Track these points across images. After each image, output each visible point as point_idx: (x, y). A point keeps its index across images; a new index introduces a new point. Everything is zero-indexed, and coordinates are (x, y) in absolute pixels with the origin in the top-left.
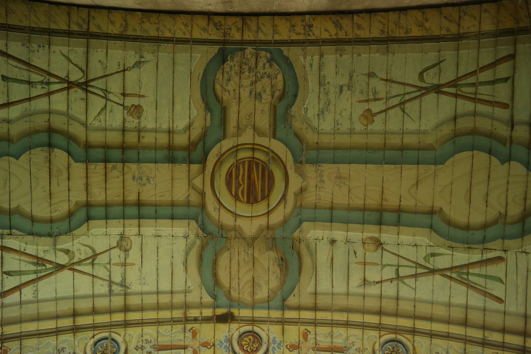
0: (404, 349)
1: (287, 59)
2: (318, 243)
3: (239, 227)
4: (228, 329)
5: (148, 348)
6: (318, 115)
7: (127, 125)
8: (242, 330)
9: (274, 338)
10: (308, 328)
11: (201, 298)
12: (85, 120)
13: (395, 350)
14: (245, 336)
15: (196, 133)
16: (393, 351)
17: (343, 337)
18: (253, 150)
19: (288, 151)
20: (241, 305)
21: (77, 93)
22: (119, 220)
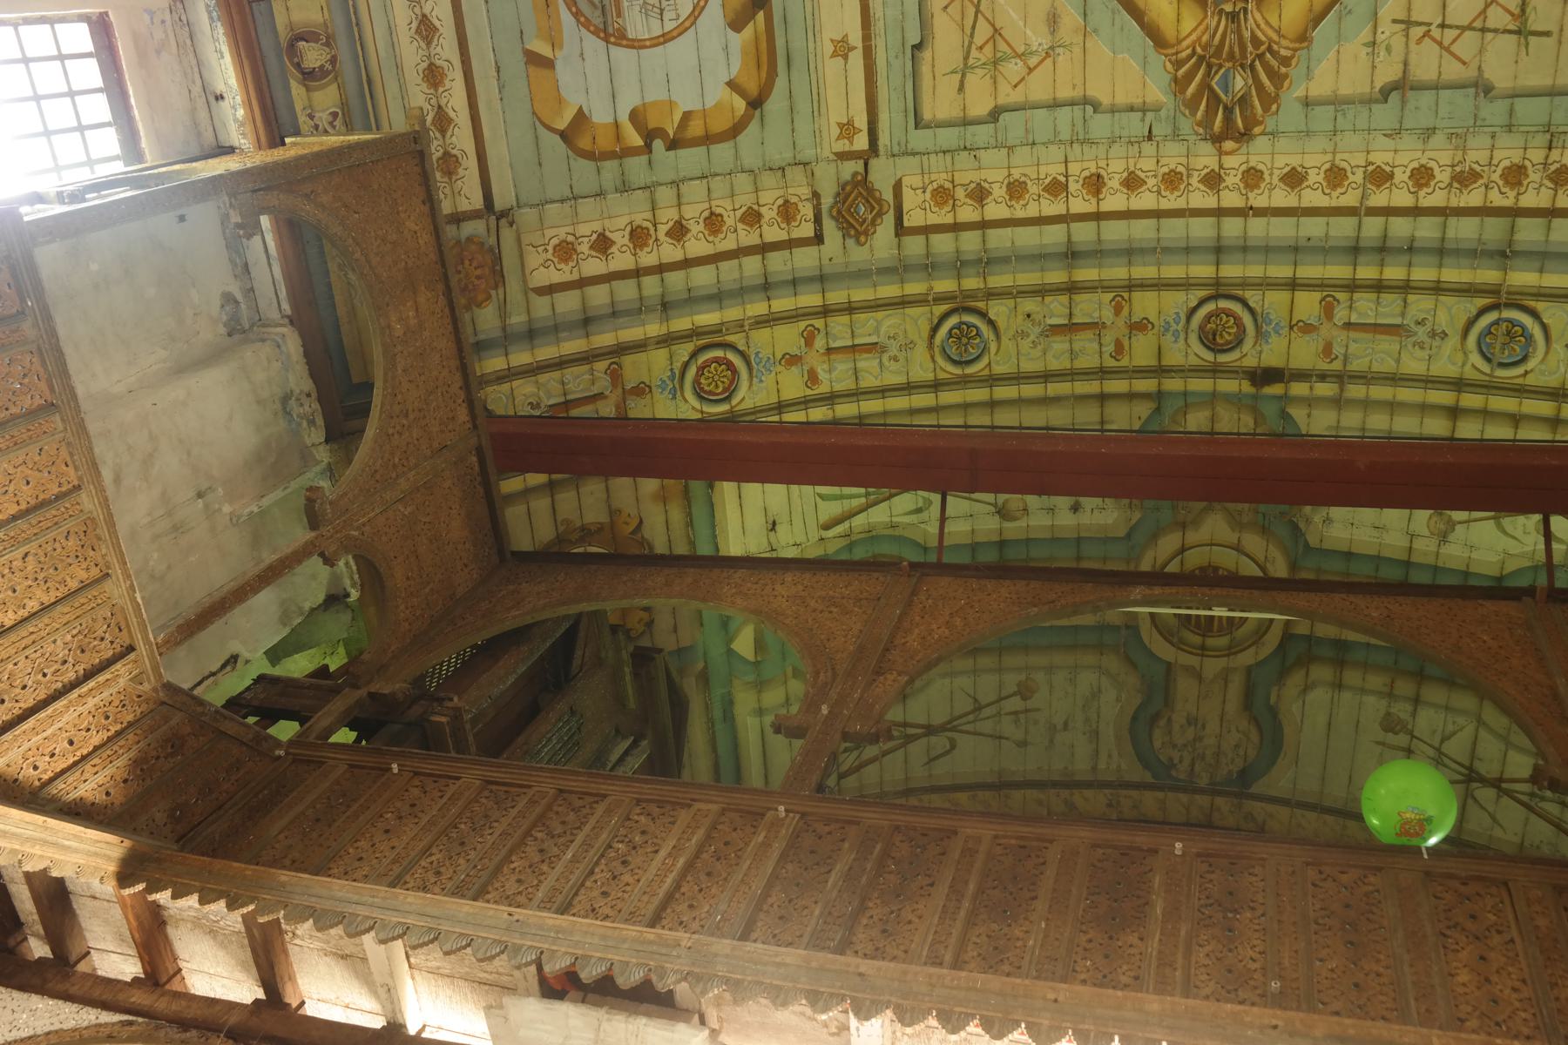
0: (949, 353)
1: (1147, 766)
3: (1233, 531)
4: (1263, 356)
5: (1422, 332)
6: (1100, 691)
7: (1409, 707)
11: (1309, 416)
12: (1480, 729)
14: (1230, 342)
15: (1296, 680)
18: (1203, 647)
19: (1147, 644)
21: (1487, 768)
22: (1447, 566)
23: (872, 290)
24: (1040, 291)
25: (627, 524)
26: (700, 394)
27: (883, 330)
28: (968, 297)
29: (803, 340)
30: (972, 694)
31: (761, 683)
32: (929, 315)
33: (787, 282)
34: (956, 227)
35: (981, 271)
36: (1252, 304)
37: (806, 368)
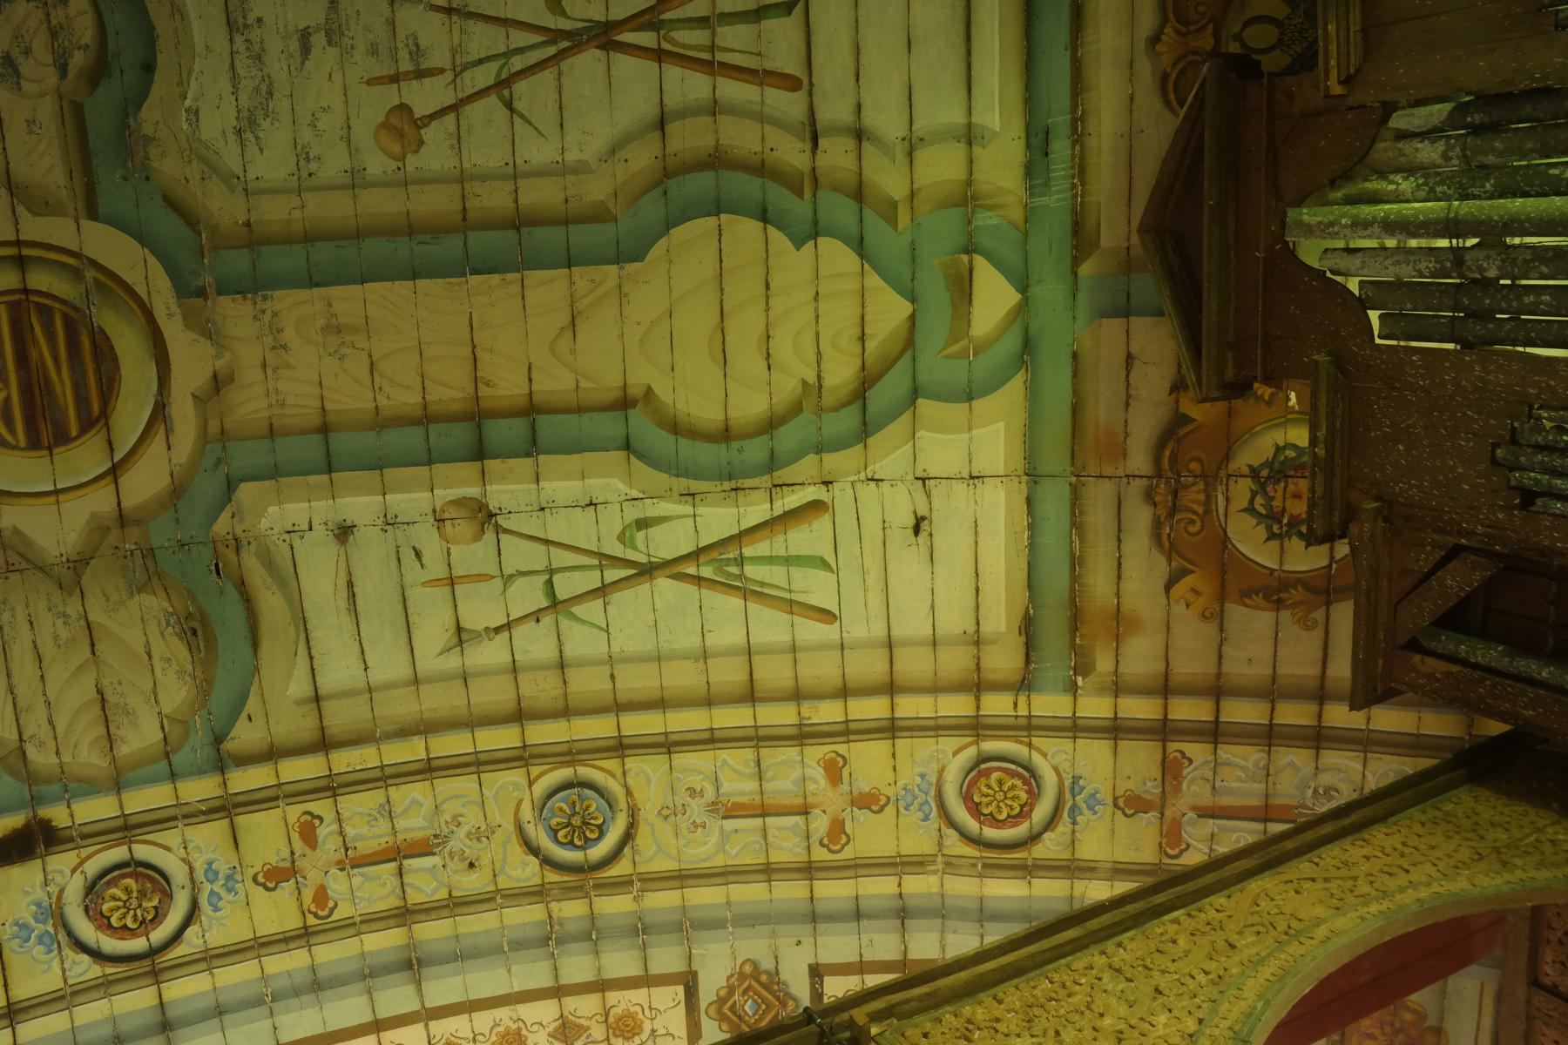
2: (297, 542)
3: (16, 532)
6: (239, 132)
8: (93, 867)
9: (210, 864)
10: (316, 807)
13: (577, 809)
14: (109, 884)
16: (573, 815)
17: (423, 811)
18: (21, 262)
19: (151, 258)
20: (73, 786)
23: (732, 898)
24: (456, 905)
25: (1193, 590)
26: (1031, 776)
27: (714, 838)
28: (574, 889)
29: (848, 830)
30: (517, 119)
31: (963, 202)
32: (637, 858)
33: (870, 917)
34: (601, 986)
35: (557, 927)
36: (85, 958)
37: (845, 787)
